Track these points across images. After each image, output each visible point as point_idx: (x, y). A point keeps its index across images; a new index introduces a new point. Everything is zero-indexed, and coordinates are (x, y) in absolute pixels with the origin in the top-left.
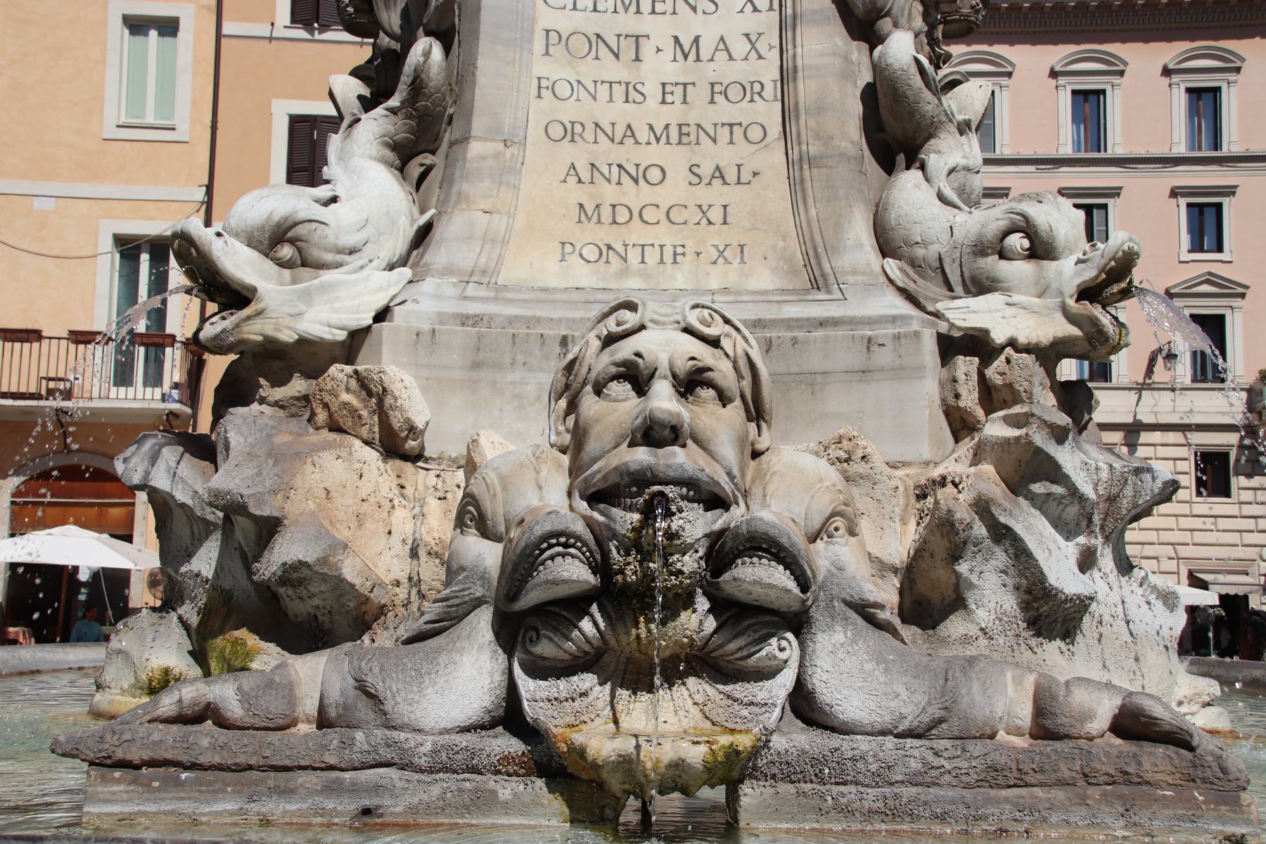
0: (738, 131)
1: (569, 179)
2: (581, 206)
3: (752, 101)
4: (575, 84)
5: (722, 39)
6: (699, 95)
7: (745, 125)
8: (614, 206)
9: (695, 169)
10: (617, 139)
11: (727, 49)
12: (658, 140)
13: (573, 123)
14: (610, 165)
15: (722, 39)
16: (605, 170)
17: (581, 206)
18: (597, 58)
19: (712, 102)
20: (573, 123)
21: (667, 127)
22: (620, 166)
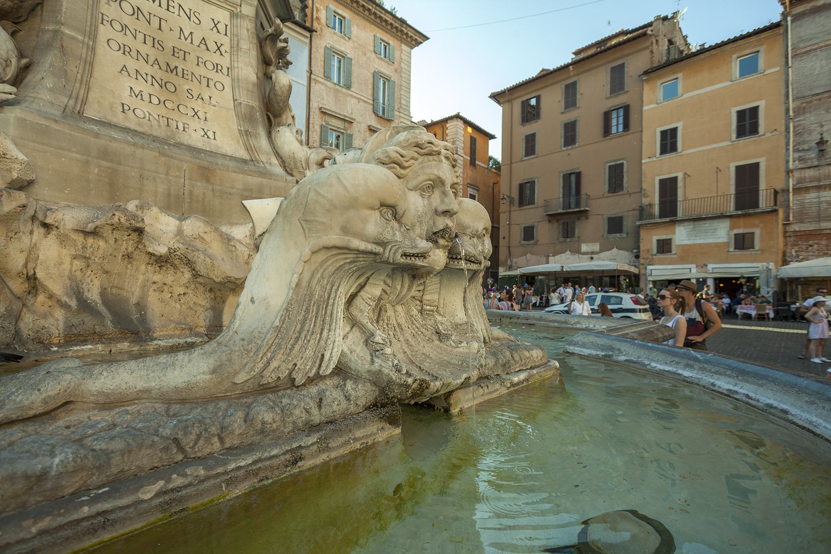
0: (211, 83)
1: (123, 72)
2: (131, 88)
3: (217, 72)
4: (124, 26)
5: (204, 39)
6: (191, 58)
7: (214, 81)
8: (150, 95)
9: (190, 91)
10: (151, 62)
11: (206, 44)
12: (172, 72)
13: (124, 45)
14: (147, 74)
15: (204, 39)
16: (144, 76)
17: (131, 88)
18: (138, 19)
19: (198, 65)
20: (124, 45)
21: (176, 67)
22: (153, 77)
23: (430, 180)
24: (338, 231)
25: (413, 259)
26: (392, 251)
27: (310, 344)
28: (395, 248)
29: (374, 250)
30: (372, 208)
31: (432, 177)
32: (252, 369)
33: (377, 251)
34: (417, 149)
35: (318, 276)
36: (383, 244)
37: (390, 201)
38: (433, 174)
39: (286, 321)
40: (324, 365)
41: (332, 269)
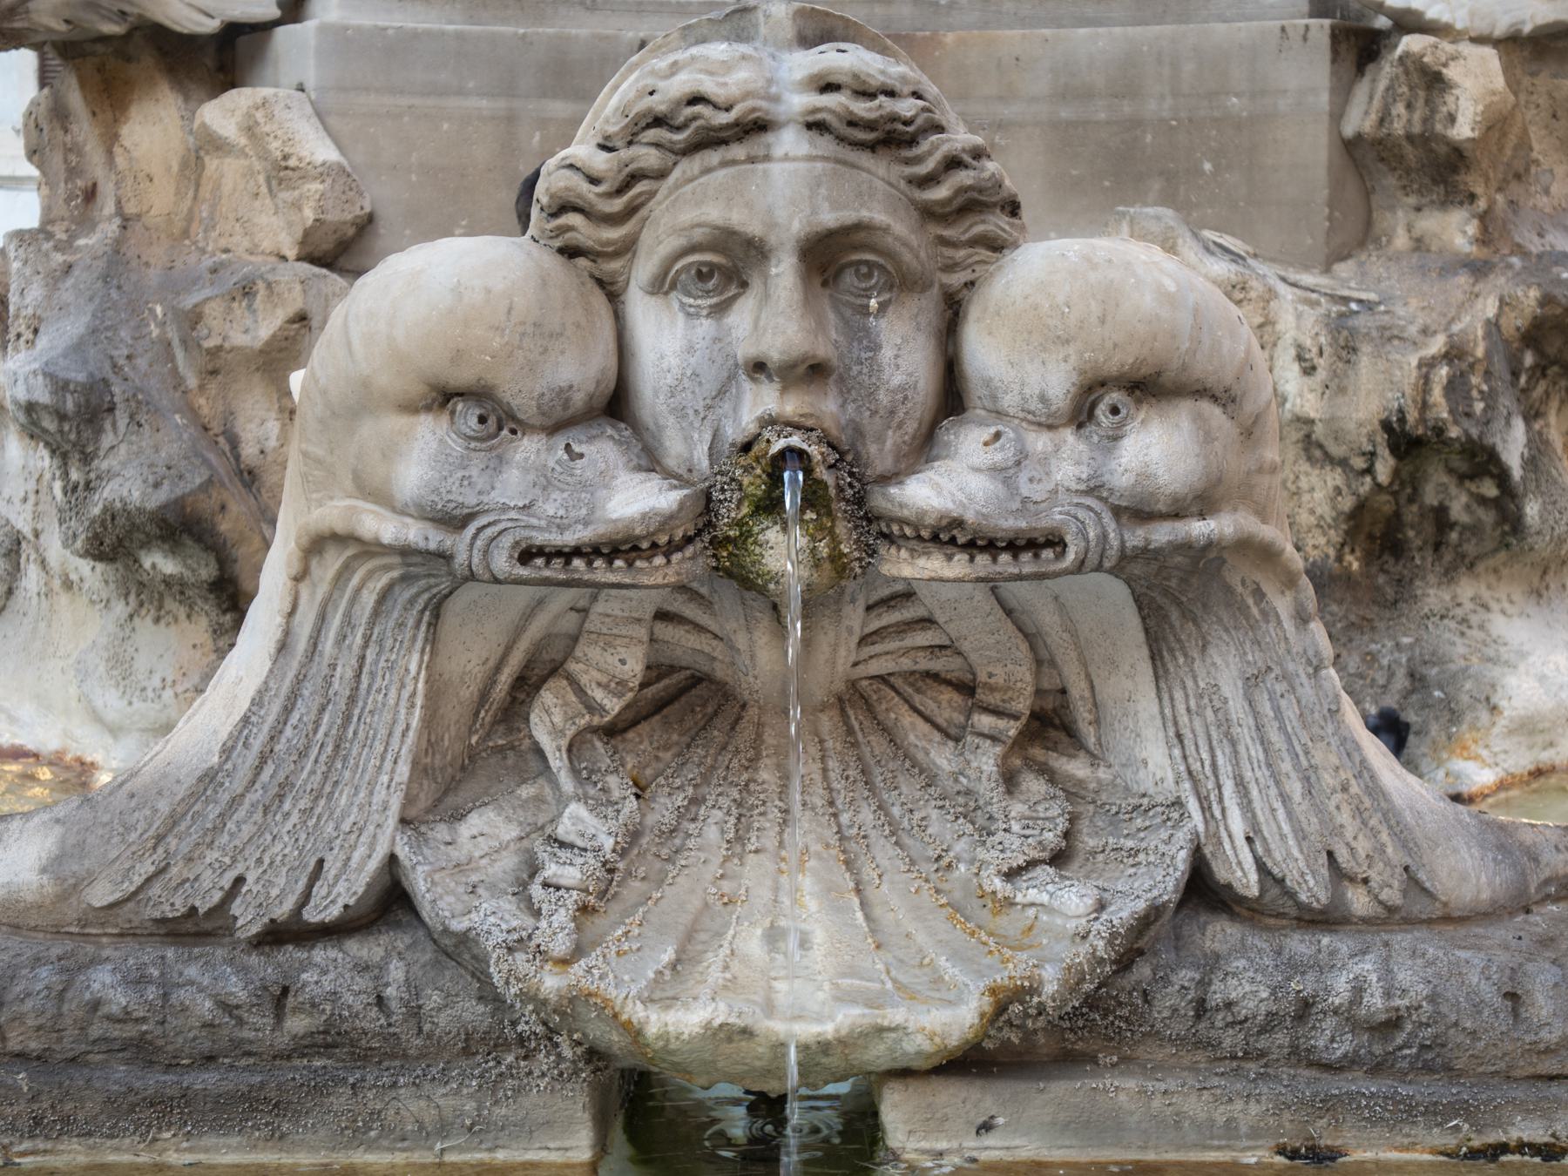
23: (693, 249)
24: (348, 484)
25: (578, 563)
26: (479, 543)
27: (289, 826)
28: (489, 532)
29: (422, 544)
30: (411, 408)
31: (698, 235)
32: (127, 874)
33: (432, 546)
34: (653, 134)
35: (335, 622)
36: (455, 521)
37: (462, 376)
38: (699, 225)
39: (235, 755)
40: (320, 890)
41: (369, 599)
